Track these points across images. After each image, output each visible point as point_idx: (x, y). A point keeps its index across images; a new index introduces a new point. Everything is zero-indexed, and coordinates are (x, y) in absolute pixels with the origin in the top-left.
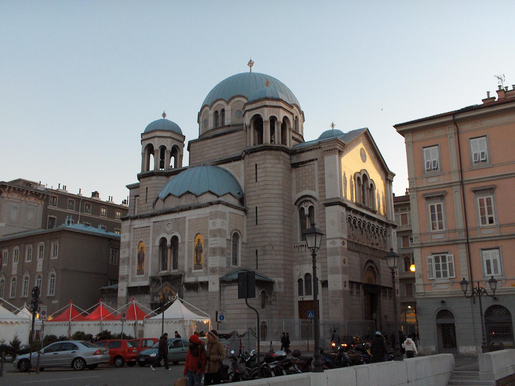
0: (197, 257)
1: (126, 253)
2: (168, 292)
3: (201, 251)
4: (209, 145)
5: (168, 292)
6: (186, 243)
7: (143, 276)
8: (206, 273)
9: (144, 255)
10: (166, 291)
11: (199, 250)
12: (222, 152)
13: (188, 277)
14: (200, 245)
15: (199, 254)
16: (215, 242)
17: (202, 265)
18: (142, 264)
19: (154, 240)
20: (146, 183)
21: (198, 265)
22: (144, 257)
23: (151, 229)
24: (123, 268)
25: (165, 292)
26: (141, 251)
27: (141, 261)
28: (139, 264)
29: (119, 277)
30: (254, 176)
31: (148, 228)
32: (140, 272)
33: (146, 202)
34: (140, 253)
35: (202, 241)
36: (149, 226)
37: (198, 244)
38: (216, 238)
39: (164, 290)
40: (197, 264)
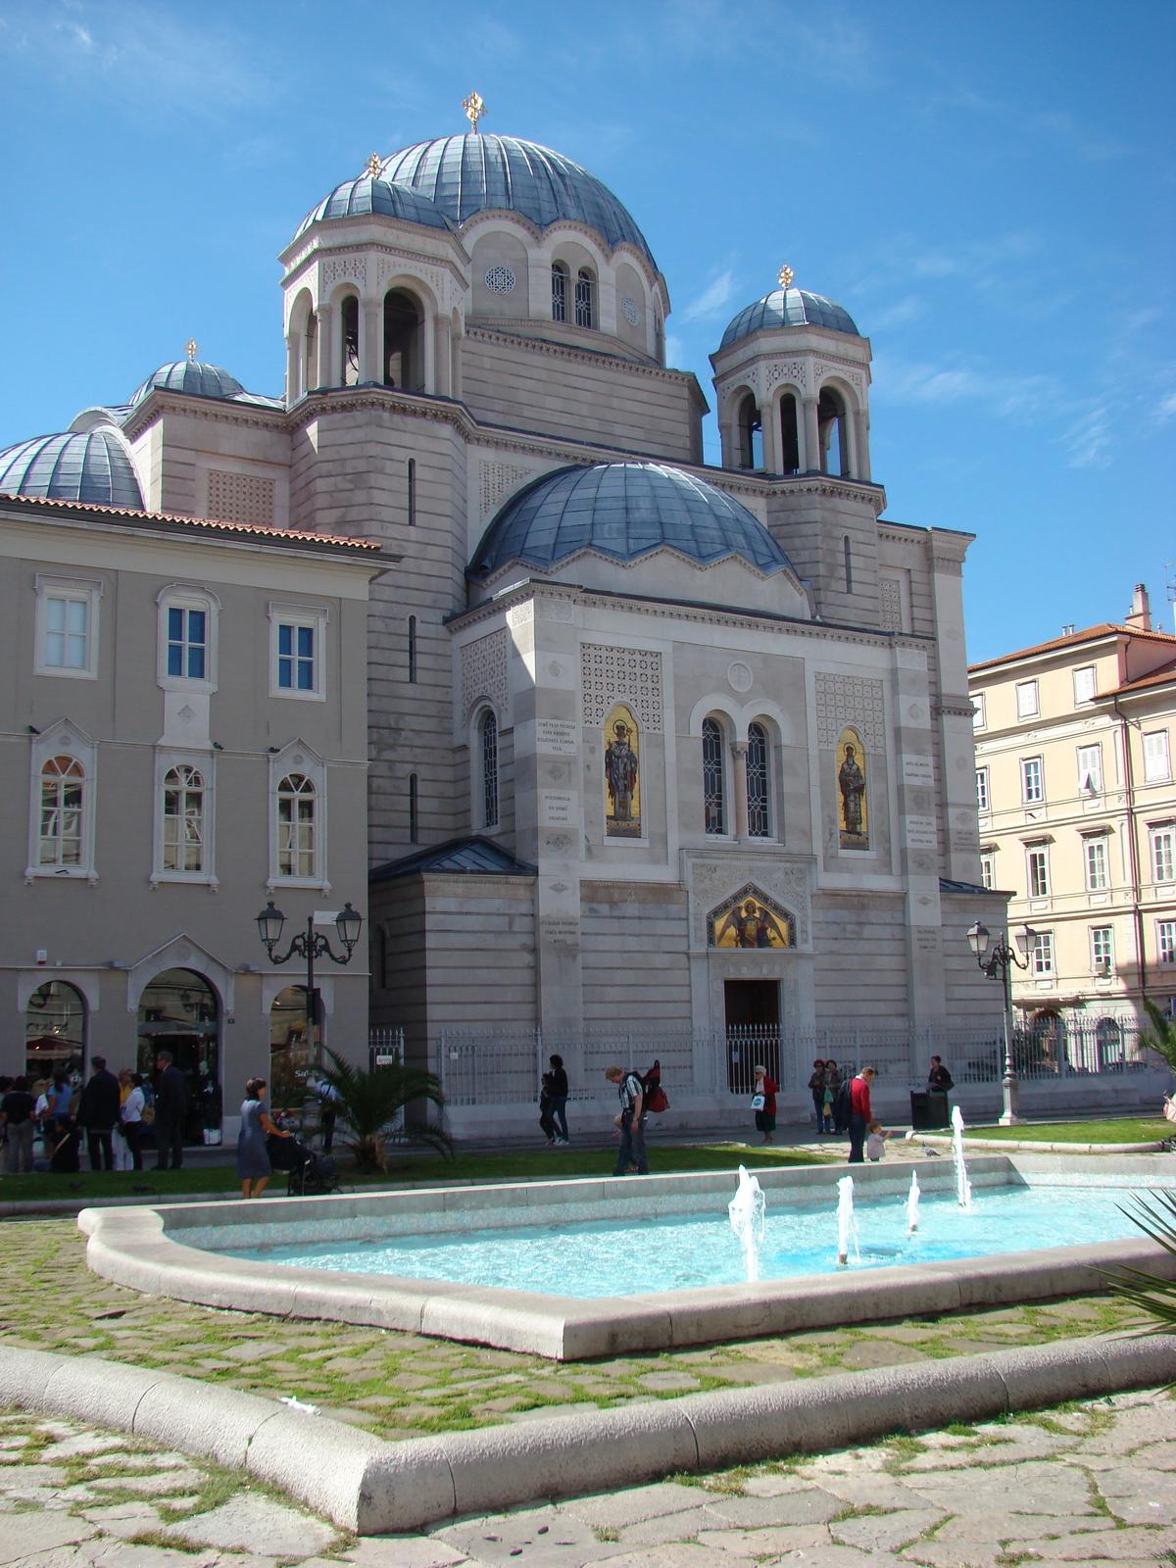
0: (846, 804)
1: (566, 738)
2: (757, 915)
3: (860, 790)
4: (544, 375)
5: (757, 915)
6: (813, 752)
7: (644, 843)
8: (885, 866)
9: (632, 759)
10: (750, 908)
11: (851, 785)
12: (594, 425)
13: (826, 869)
14: (855, 767)
15: (852, 798)
16: (921, 771)
17: (864, 836)
18: (625, 798)
19: (683, 713)
20: (406, 439)
21: (853, 835)
22: (633, 772)
23: (668, 667)
24: (559, 798)
25: (744, 914)
26: (619, 743)
27: (621, 784)
28: (612, 794)
29: (541, 836)
30: (842, 572)
31: (649, 659)
32: (623, 824)
33: (411, 522)
34: (617, 752)
35: (858, 760)
36: (658, 654)
37: (847, 762)
38: (922, 757)
39: (740, 908)
40: (849, 832)
